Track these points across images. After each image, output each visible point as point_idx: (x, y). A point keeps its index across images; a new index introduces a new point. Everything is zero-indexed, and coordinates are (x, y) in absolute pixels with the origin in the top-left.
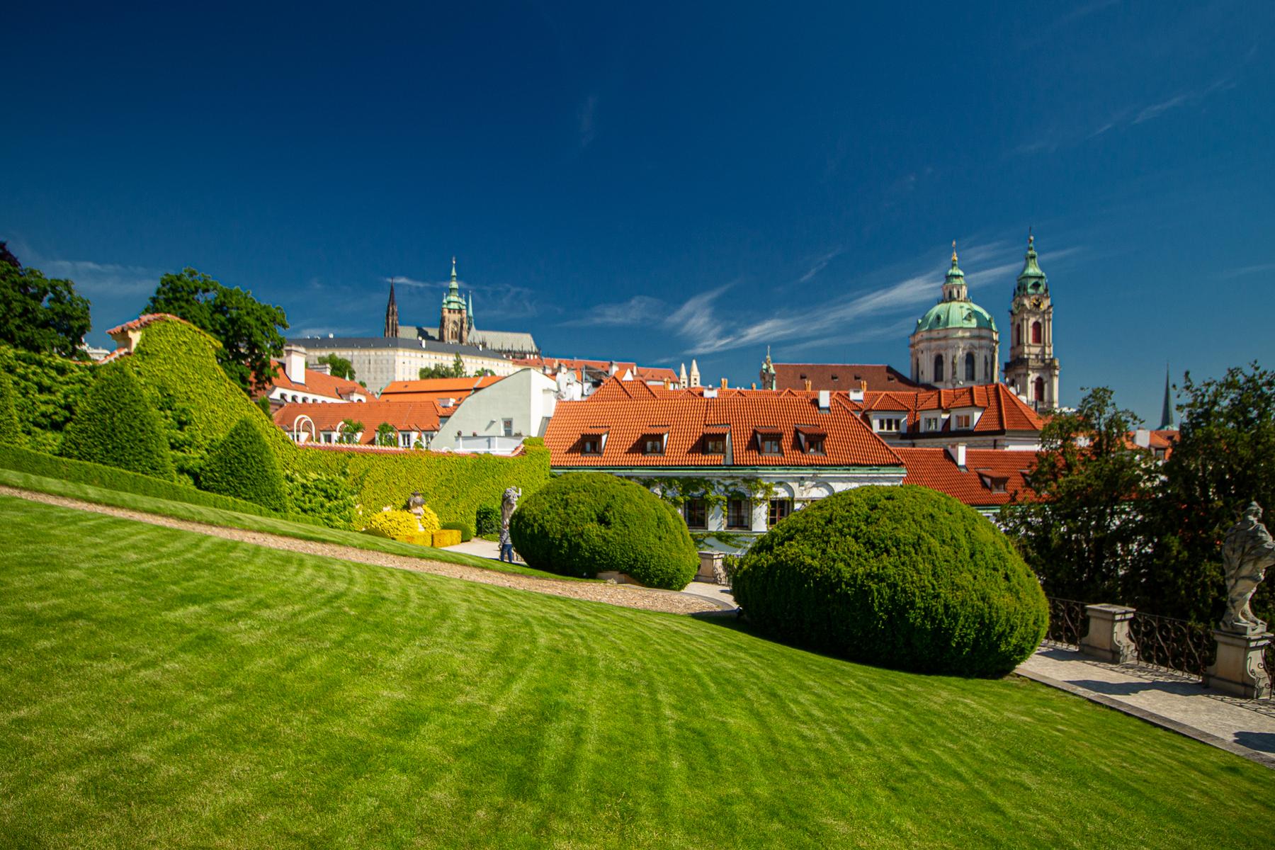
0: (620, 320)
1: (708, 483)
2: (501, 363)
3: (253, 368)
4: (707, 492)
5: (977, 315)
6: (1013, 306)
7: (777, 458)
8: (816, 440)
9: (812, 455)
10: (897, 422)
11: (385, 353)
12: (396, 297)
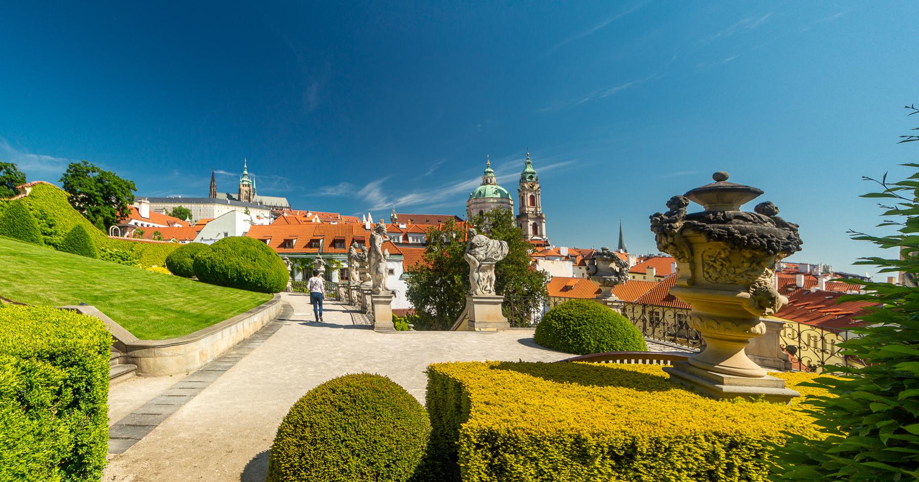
3: (118, 209)
5: (500, 191)
7: (342, 250)
11: (208, 206)
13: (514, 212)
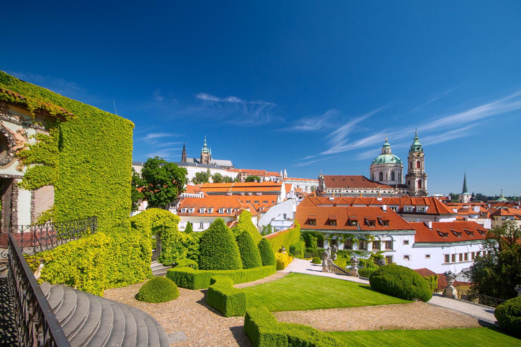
1: (353, 235)
2: (222, 171)
6: (408, 156)
8: (386, 222)
10: (395, 208)
12: (186, 149)
13: (405, 172)
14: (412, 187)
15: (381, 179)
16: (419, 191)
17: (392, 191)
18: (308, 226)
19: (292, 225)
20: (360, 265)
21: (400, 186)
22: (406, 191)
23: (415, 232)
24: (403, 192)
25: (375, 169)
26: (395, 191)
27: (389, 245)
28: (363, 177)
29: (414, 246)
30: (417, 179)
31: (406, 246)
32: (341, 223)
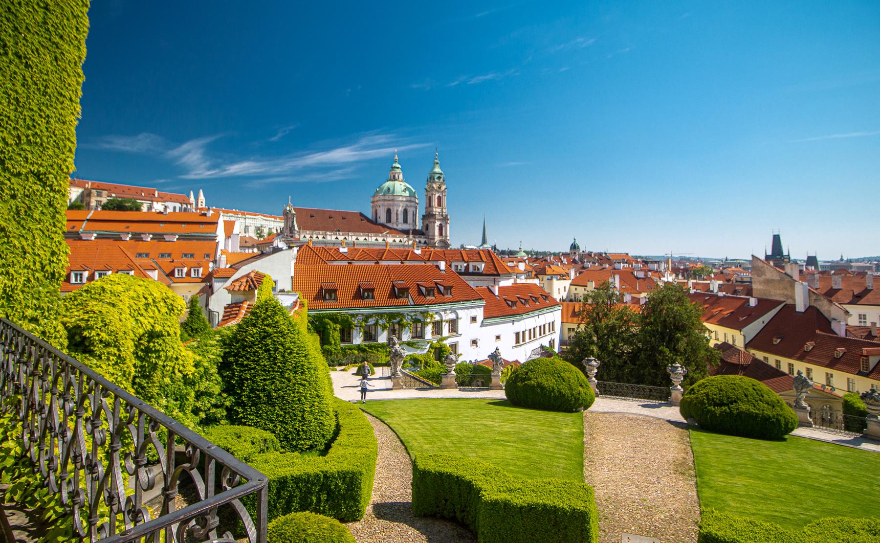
0: (128, 148)
1: (402, 315)
4: (401, 320)
6: (427, 187)
8: (448, 288)
9: (448, 296)
13: (421, 212)
14: (431, 234)
15: (389, 220)
16: (441, 241)
17: (406, 239)
18: (321, 303)
19: (295, 303)
20: (414, 366)
21: (416, 233)
22: (423, 240)
23: (483, 303)
24: (420, 242)
25: (379, 203)
26: (409, 240)
27: (454, 325)
28: (361, 214)
29: (482, 325)
30: (438, 223)
31: (474, 325)
32: (381, 294)
